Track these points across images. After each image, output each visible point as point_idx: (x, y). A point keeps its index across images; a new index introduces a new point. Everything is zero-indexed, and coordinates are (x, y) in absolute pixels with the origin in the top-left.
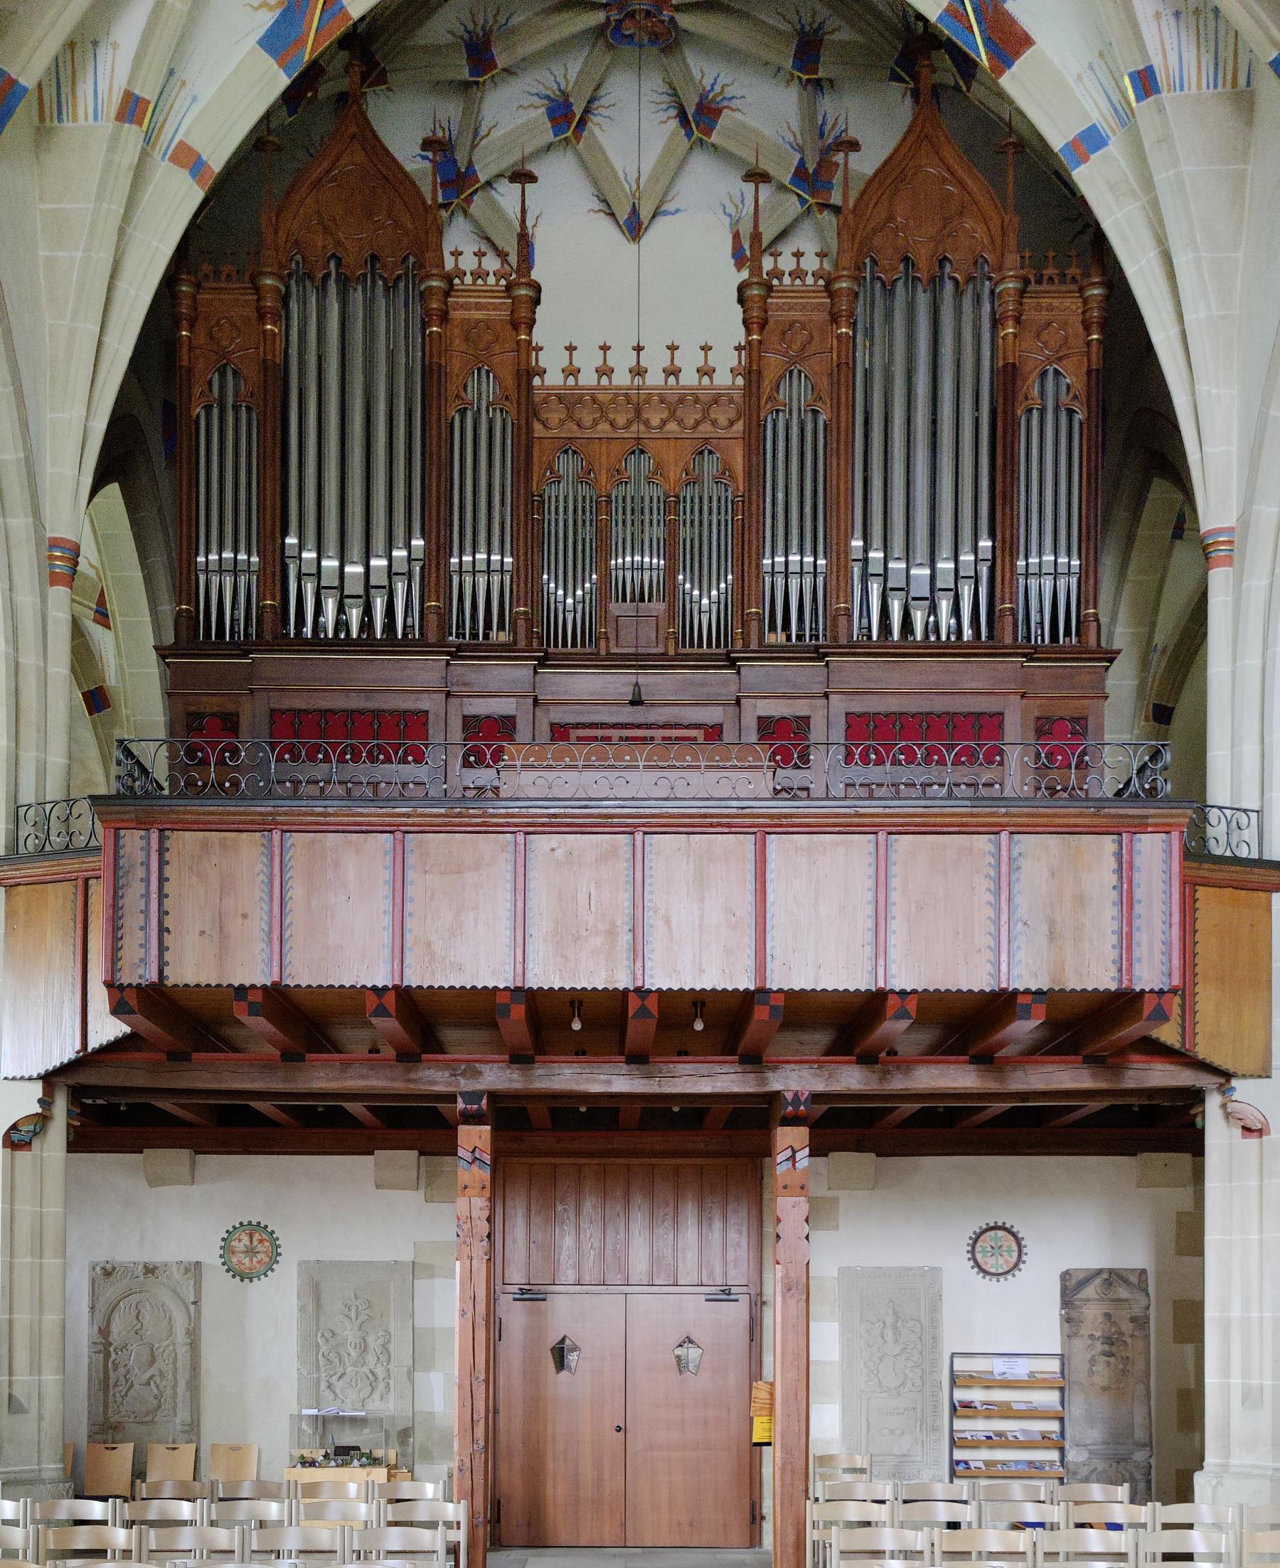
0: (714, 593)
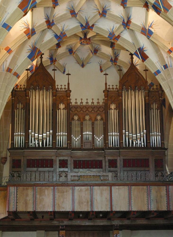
0: (100, 138)
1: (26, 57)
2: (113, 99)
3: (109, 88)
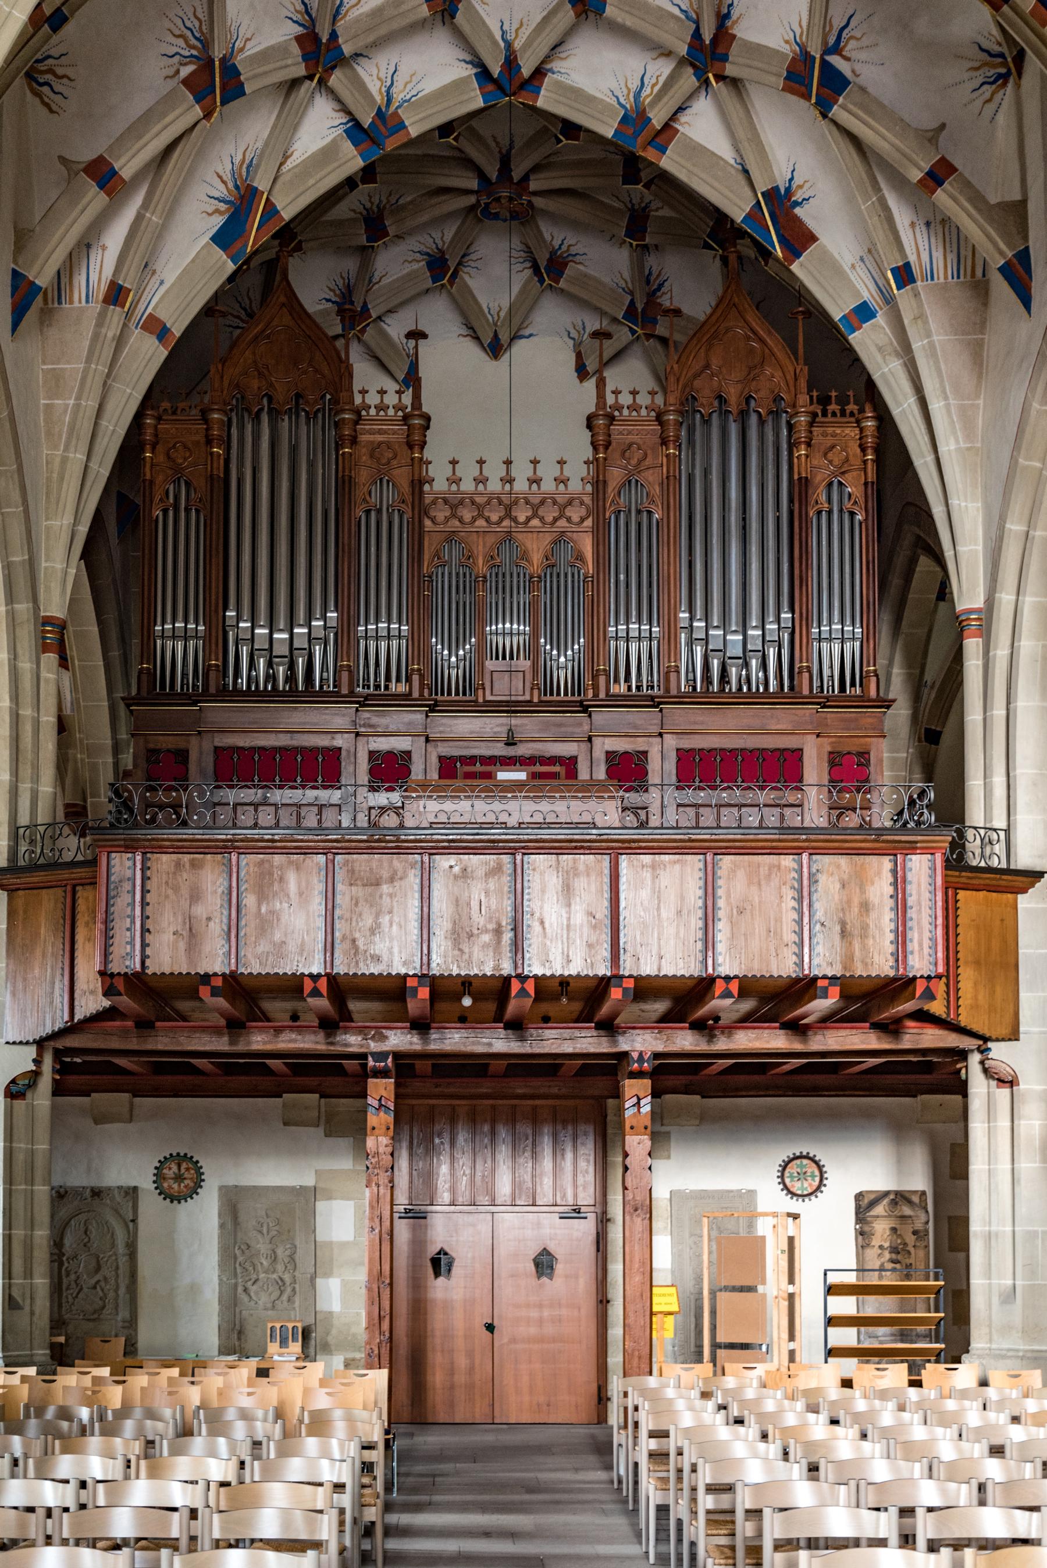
1: (206, 239)
2: (634, 462)
3: (619, 408)
